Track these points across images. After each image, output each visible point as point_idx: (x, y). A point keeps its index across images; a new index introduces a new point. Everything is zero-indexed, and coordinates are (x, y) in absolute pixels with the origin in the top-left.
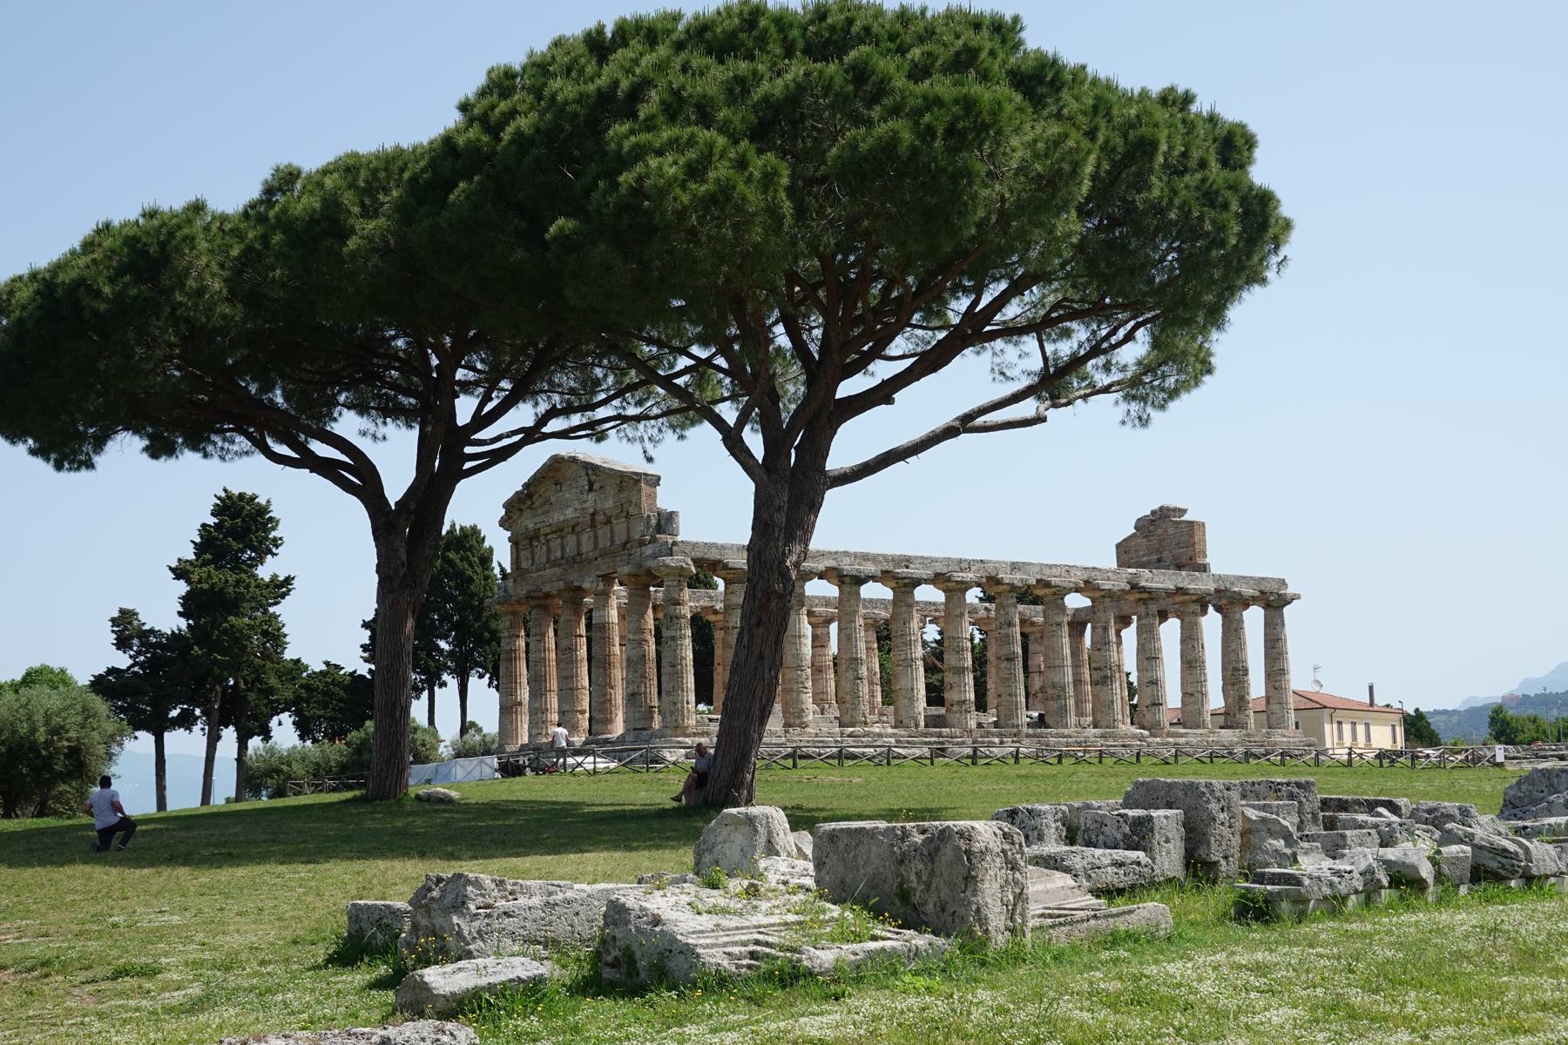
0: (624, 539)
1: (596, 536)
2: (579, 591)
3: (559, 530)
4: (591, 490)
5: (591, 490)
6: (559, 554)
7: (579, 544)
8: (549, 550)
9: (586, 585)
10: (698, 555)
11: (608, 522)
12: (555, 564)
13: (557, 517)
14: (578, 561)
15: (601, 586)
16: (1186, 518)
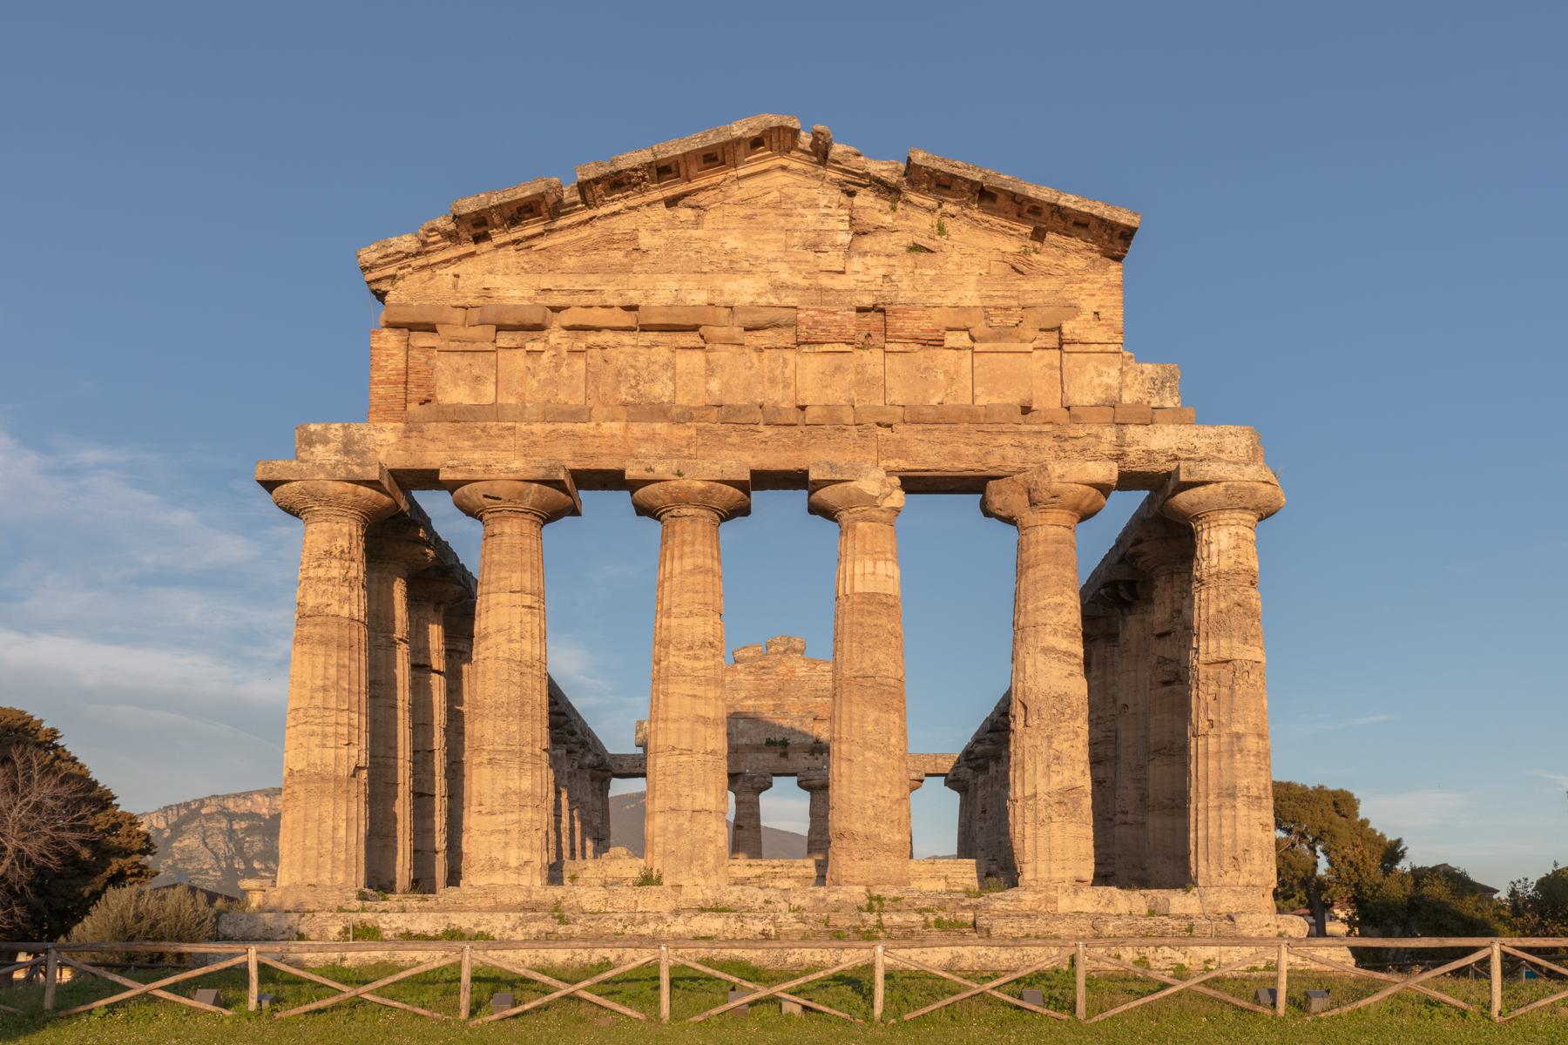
0: (1014, 398)
13: (662, 292)
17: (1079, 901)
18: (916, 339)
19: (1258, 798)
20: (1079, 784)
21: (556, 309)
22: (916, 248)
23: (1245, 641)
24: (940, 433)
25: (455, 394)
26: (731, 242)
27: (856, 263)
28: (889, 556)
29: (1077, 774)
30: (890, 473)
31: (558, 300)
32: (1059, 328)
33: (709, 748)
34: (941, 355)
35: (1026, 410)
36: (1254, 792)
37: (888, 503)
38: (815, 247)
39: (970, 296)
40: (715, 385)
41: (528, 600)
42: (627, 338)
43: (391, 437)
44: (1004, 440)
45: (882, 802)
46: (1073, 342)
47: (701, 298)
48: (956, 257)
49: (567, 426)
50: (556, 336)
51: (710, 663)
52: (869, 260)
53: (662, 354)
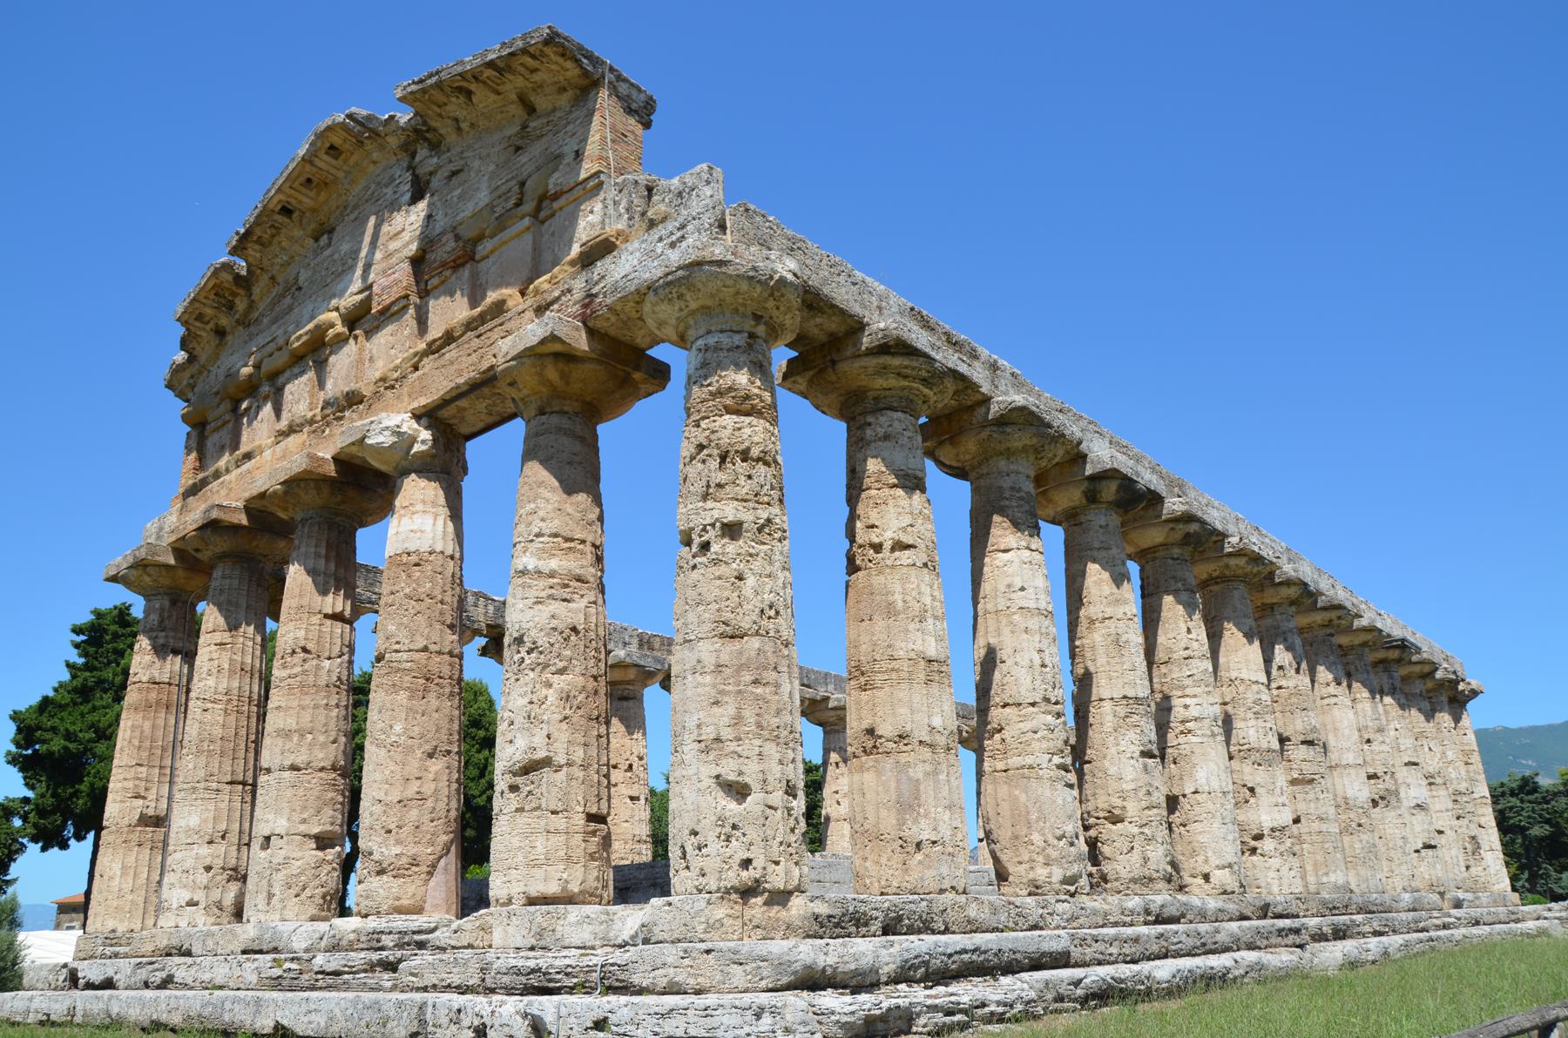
17: (511, 929)
18: (444, 265)
19: (718, 740)
20: (541, 754)
22: (454, 173)
23: (705, 497)
24: (451, 353)
28: (419, 507)
29: (539, 740)
30: (417, 417)
33: (287, 763)
36: (709, 733)
37: (417, 448)
44: (495, 335)
45: (378, 809)
48: (476, 164)
49: (248, 465)
51: (298, 669)
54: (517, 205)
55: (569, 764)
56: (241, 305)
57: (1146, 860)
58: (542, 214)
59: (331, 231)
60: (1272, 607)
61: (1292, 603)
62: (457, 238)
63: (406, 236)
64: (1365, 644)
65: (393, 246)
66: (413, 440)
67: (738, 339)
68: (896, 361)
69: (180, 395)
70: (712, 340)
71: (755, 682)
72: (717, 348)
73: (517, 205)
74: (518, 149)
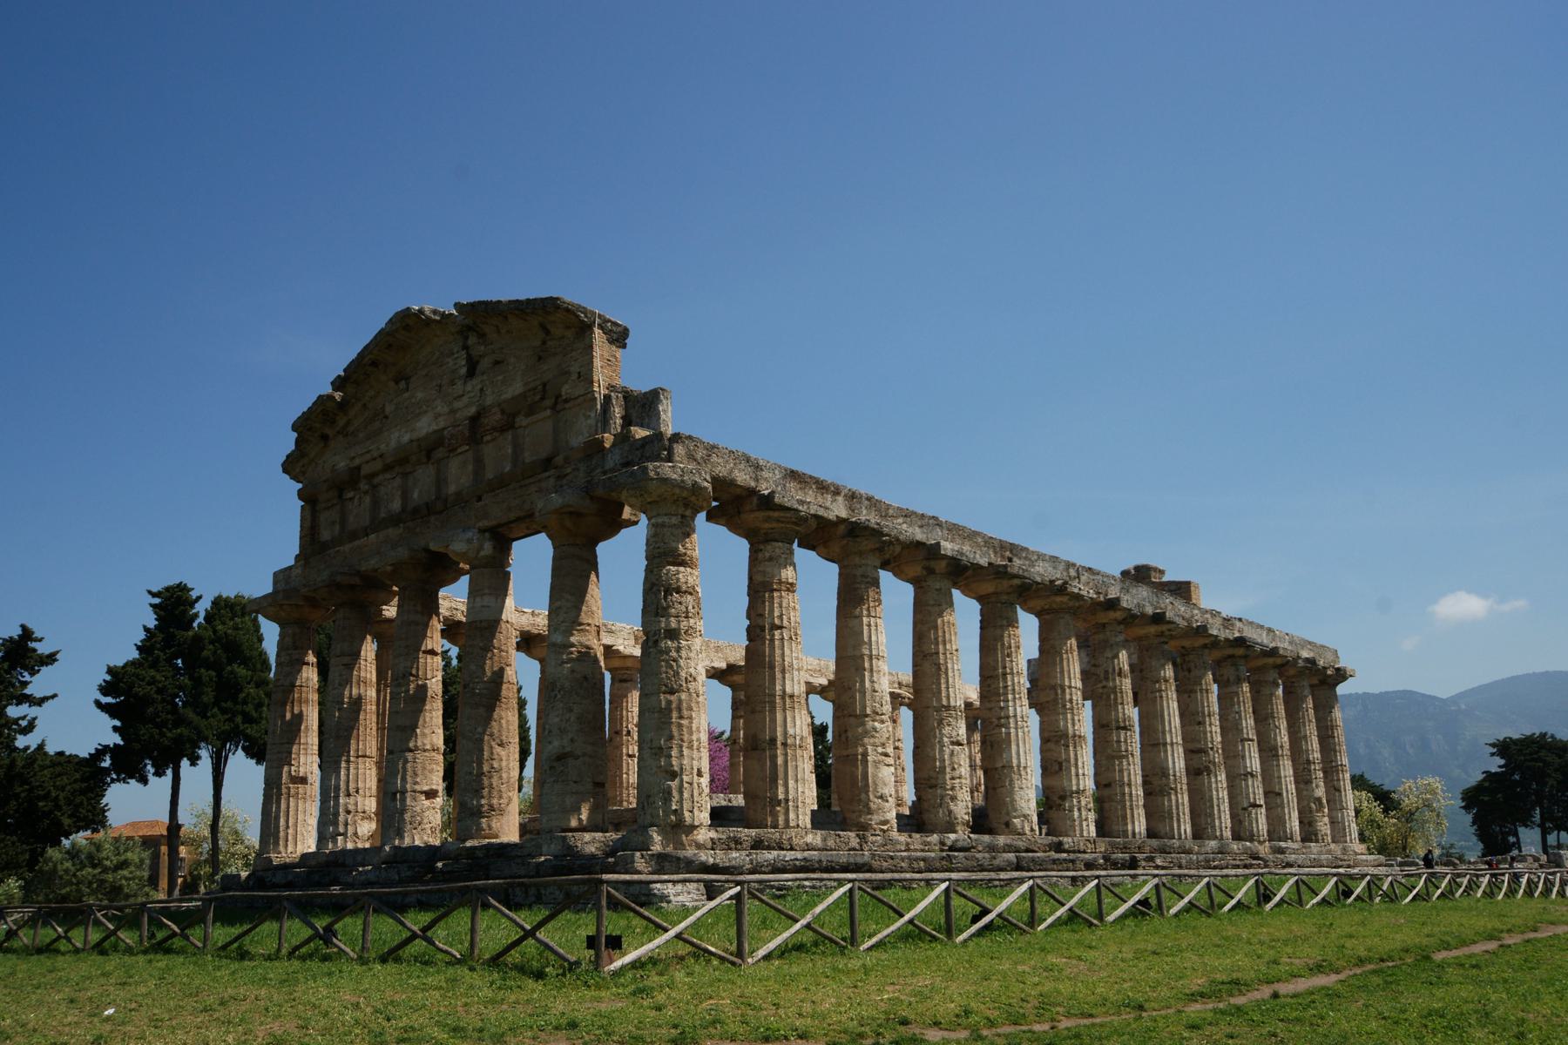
1: (479, 463)
2: (440, 569)
3: (401, 463)
4: (471, 373)
5: (471, 373)
6: (396, 505)
7: (440, 482)
8: (376, 504)
9: (458, 546)
10: (722, 471)
11: (508, 425)
12: (395, 520)
13: (397, 438)
14: (438, 509)
15: (488, 549)
16: (1165, 579)
18: (494, 429)
21: (358, 468)
22: (497, 363)
23: (657, 615)
25: (325, 535)
26: (420, 395)
27: (469, 388)
30: (482, 531)
31: (357, 462)
32: (558, 396)
34: (509, 436)
35: (547, 463)
37: (482, 553)
38: (452, 383)
39: (516, 388)
40: (416, 495)
41: (346, 660)
42: (388, 476)
43: (299, 571)
46: (566, 401)
47: (406, 438)
49: (357, 543)
50: (364, 486)
52: (475, 381)
53: (398, 481)
54: (543, 399)
55: (584, 755)
56: (341, 422)
57: (950, 812)
58: (559, 407)
59: (407, 379)
60: (1104, 625)
61: (1120, 623)
62: (503, 412)
63: (465, 399)
64: (1205, 646)
65: (457, 405)
66: (481, 548)
67: (674, 520)
68: (776, 514)
69: (295, 478)
70: (660, 520)
71: (681, 717)
72: (663, 525)
73: (543, 399)
74: (540, 358)
